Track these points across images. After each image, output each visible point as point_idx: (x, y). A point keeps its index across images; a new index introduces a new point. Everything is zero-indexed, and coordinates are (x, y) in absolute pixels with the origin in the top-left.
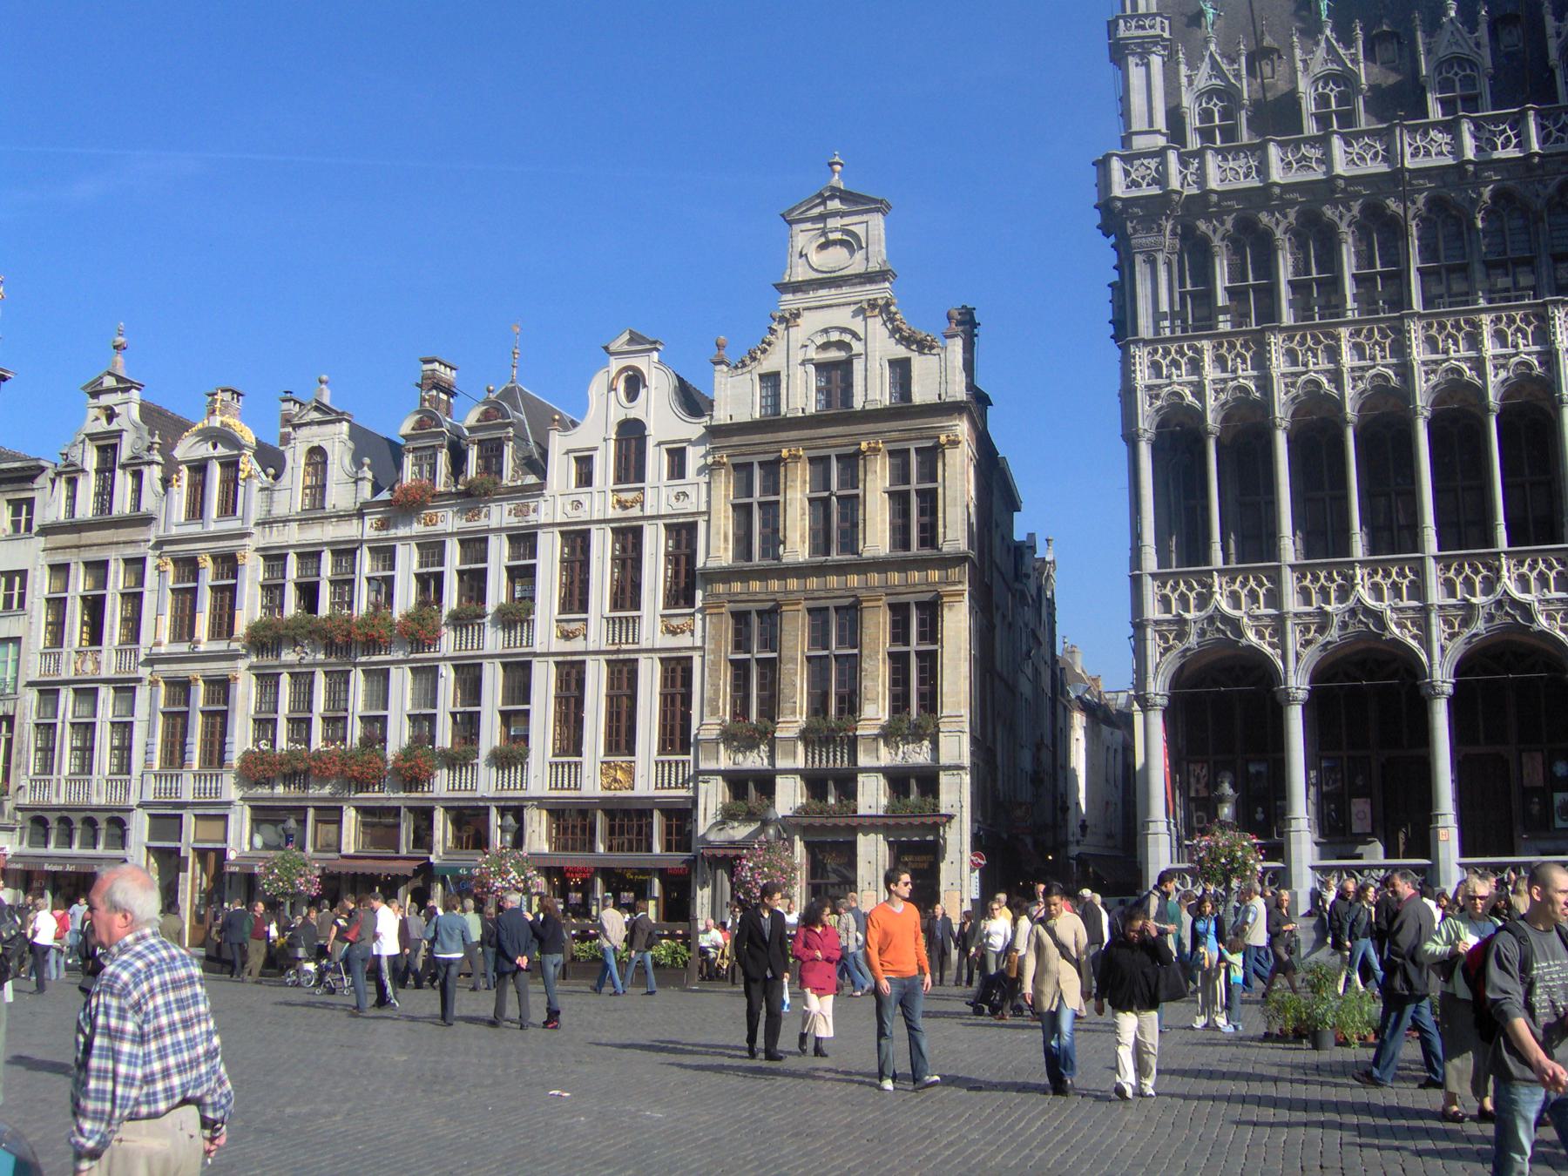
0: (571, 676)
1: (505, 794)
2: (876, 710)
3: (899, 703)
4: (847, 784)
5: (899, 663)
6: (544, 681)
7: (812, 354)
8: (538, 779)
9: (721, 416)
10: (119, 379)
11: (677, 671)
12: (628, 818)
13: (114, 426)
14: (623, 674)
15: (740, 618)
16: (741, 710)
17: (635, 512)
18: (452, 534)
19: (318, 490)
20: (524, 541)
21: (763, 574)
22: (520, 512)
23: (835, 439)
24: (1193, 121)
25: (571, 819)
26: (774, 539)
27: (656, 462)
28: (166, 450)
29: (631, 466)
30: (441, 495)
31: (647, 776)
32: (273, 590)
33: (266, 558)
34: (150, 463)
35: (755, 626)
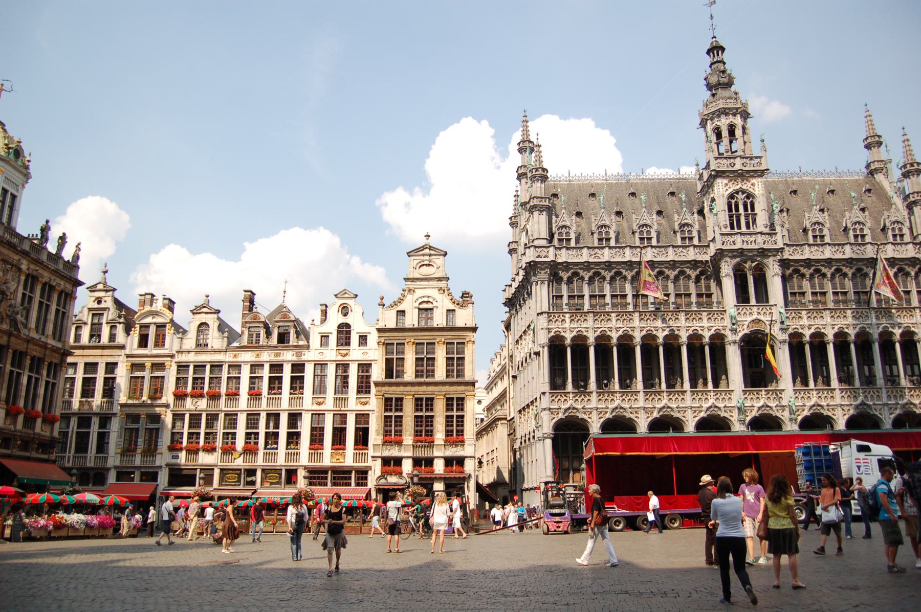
1: (289, 464)
2: (439, 435)
3: (448, 433)
4: (430, 462)
5: (449, 419)
11: (362, 418)
12: (341, 475)
13: (103, 305)
15: (387, 400)
16: (387, 433)
17: (346, 358)
23: (425, 337)
25: (317, 475)
30: (262, 346)
31: (349, 458)
34: (120, 323)
35: (392, 404)
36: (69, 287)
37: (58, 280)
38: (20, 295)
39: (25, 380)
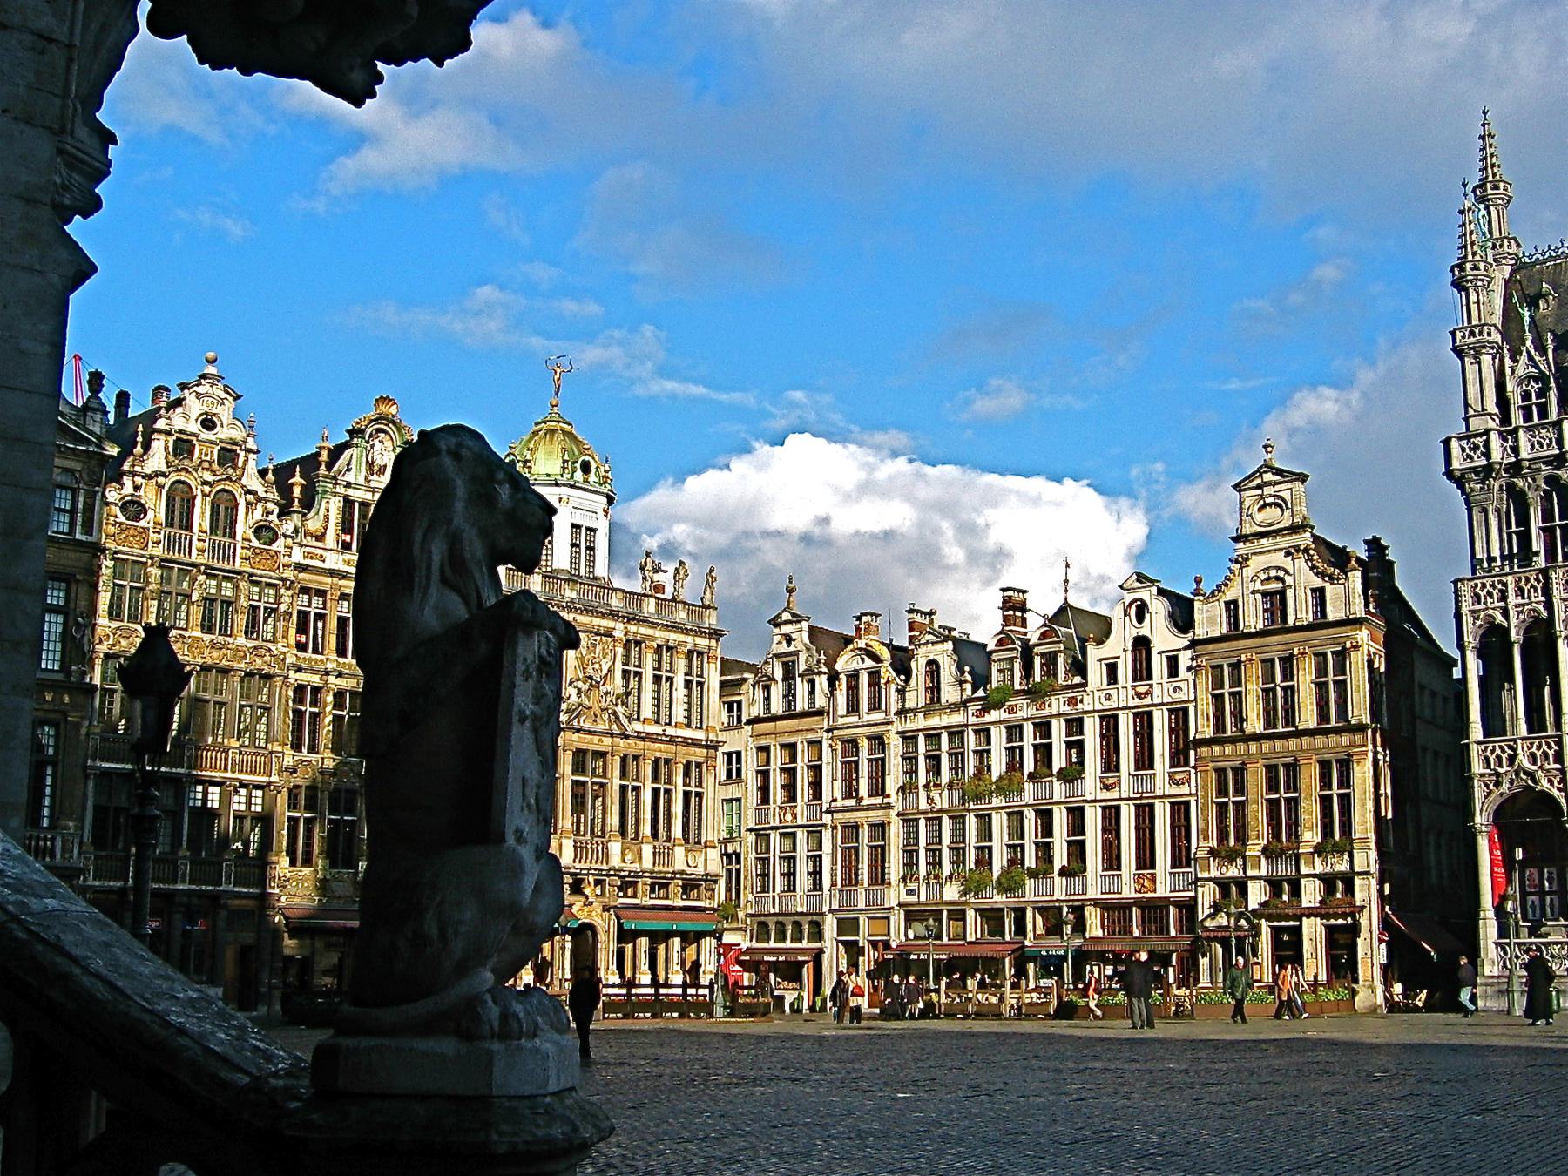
0: (1111, 816)
2: (1311, 836)
6: (1093, 819)
7: (1258, 586)
8: (1094, 884)
9: (1201, 631)
10: (794, 615)
11: (1180, 810)
12: (1154, 911)
13: (792, 648)
14: (1145, 815)
15: (1221, 773)
16: (1223, 835)
17: (1147, 701)
18: (1027, 719)
19: (934, 689)
20: (1075, 724)
21: (1233, 741)
22: (1072, 702)
24: (1515, 401)
25: (1115, 911)
26: (1240, 718)
27: (1159, 665)
28: (830, 664)
29: (1142, 671)
32: (910, 760)
33: (904, 738)
35: (1230, 779)
36: (703, 642)
37: (682, 637)
38: (618, 675)
39: (647, 796)
